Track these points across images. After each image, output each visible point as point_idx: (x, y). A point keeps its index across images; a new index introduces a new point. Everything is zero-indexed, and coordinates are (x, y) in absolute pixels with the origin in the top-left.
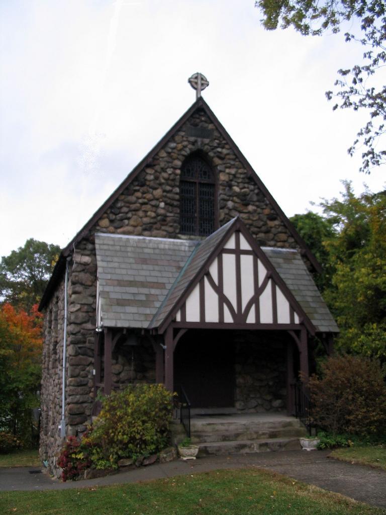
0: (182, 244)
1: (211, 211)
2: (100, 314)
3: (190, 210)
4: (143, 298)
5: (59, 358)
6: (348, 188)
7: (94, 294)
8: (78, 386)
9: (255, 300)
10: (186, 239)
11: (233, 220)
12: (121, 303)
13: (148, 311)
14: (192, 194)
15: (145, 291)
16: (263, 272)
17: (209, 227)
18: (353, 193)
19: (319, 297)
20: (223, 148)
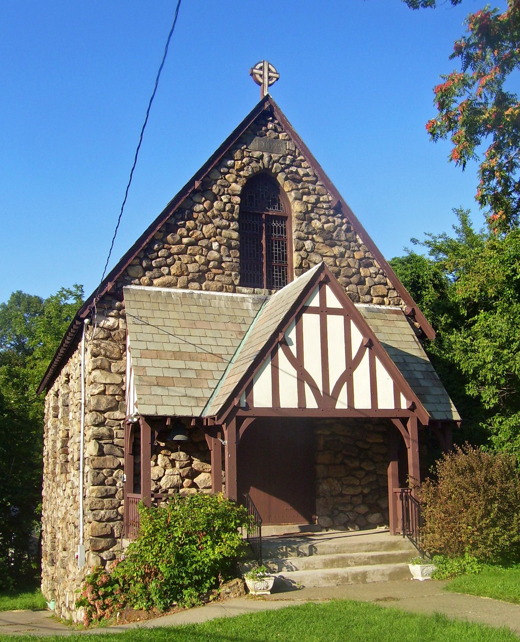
0: (243, 300)
1: (283, 255)
2: (132, 397)
3: (254, 253)
4: (192, 375)
5: (72, 459)
6: (464, 221)
7: (122, 370)
8: (103, 497)
9: (347, 378)
10: (249, 293)
11: (314, 269)
12: (161, 382)
13: (197, 393)
14: (257, 231)
15: (195, 365)
16: (357, 338)
17: (280, 275)
18: (472, 228)
19: (432, 372)
20: (300, 166)
